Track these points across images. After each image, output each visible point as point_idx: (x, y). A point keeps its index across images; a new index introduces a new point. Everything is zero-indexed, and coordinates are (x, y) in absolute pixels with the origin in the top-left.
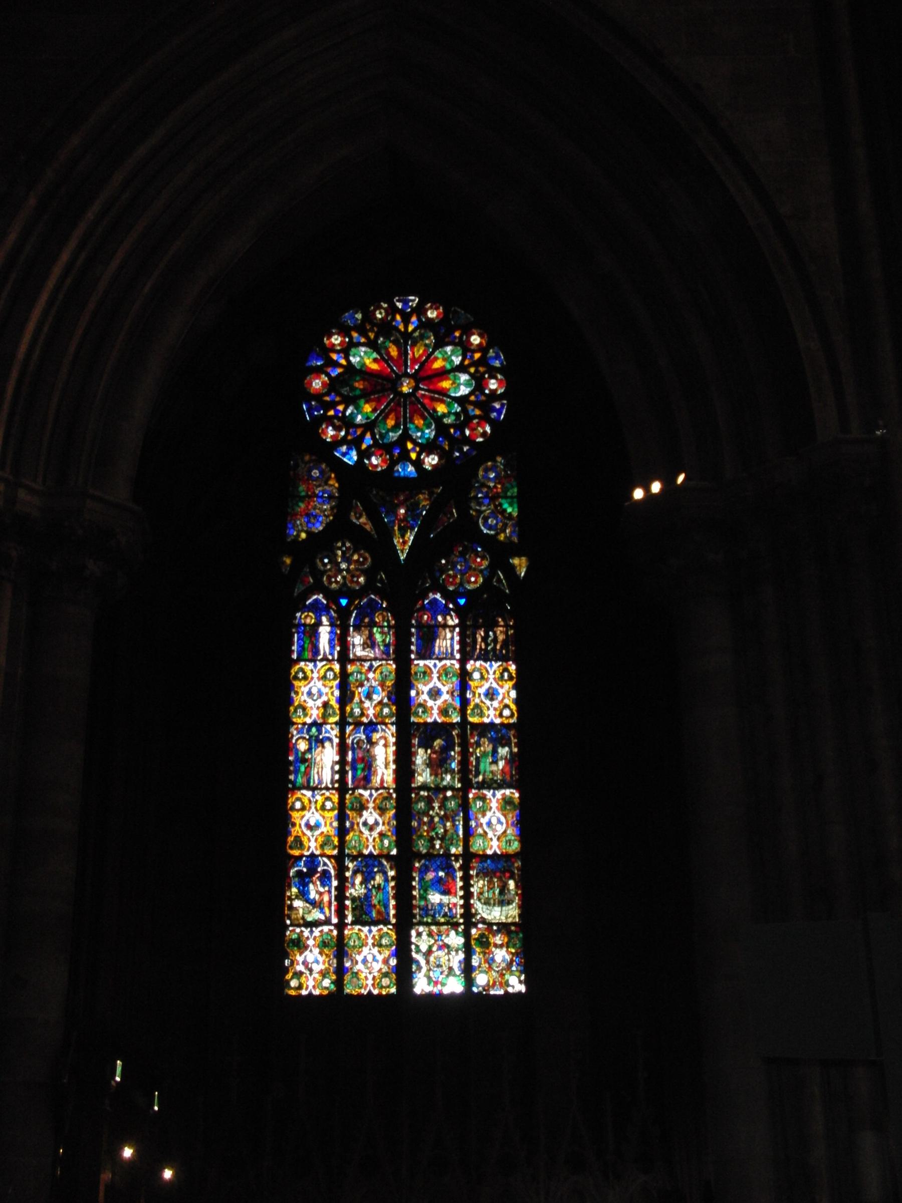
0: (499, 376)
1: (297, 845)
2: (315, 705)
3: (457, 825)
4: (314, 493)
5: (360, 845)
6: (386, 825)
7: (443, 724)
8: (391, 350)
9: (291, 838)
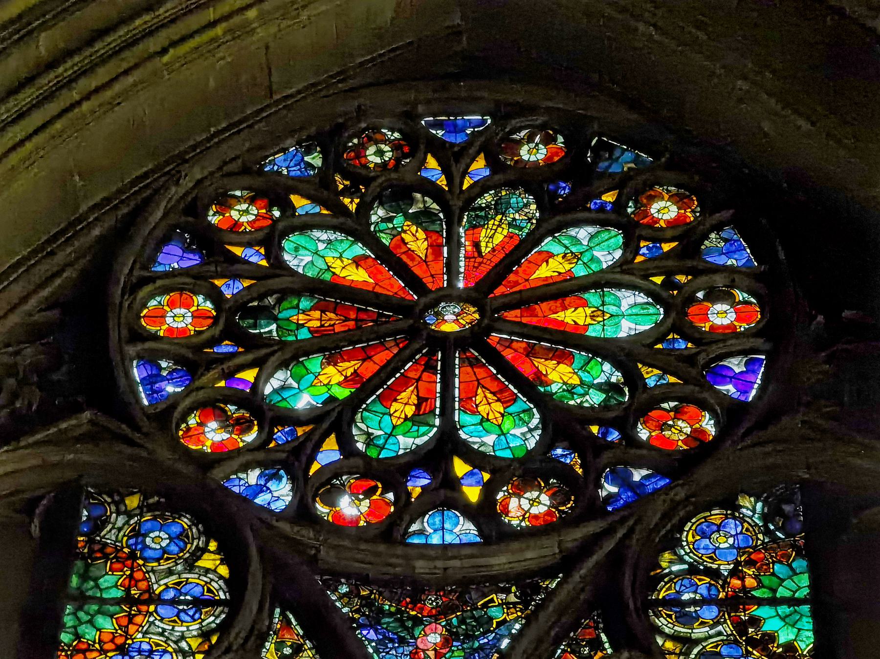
0: (740, 296)
4: (149, 590)
8: (407, 237)
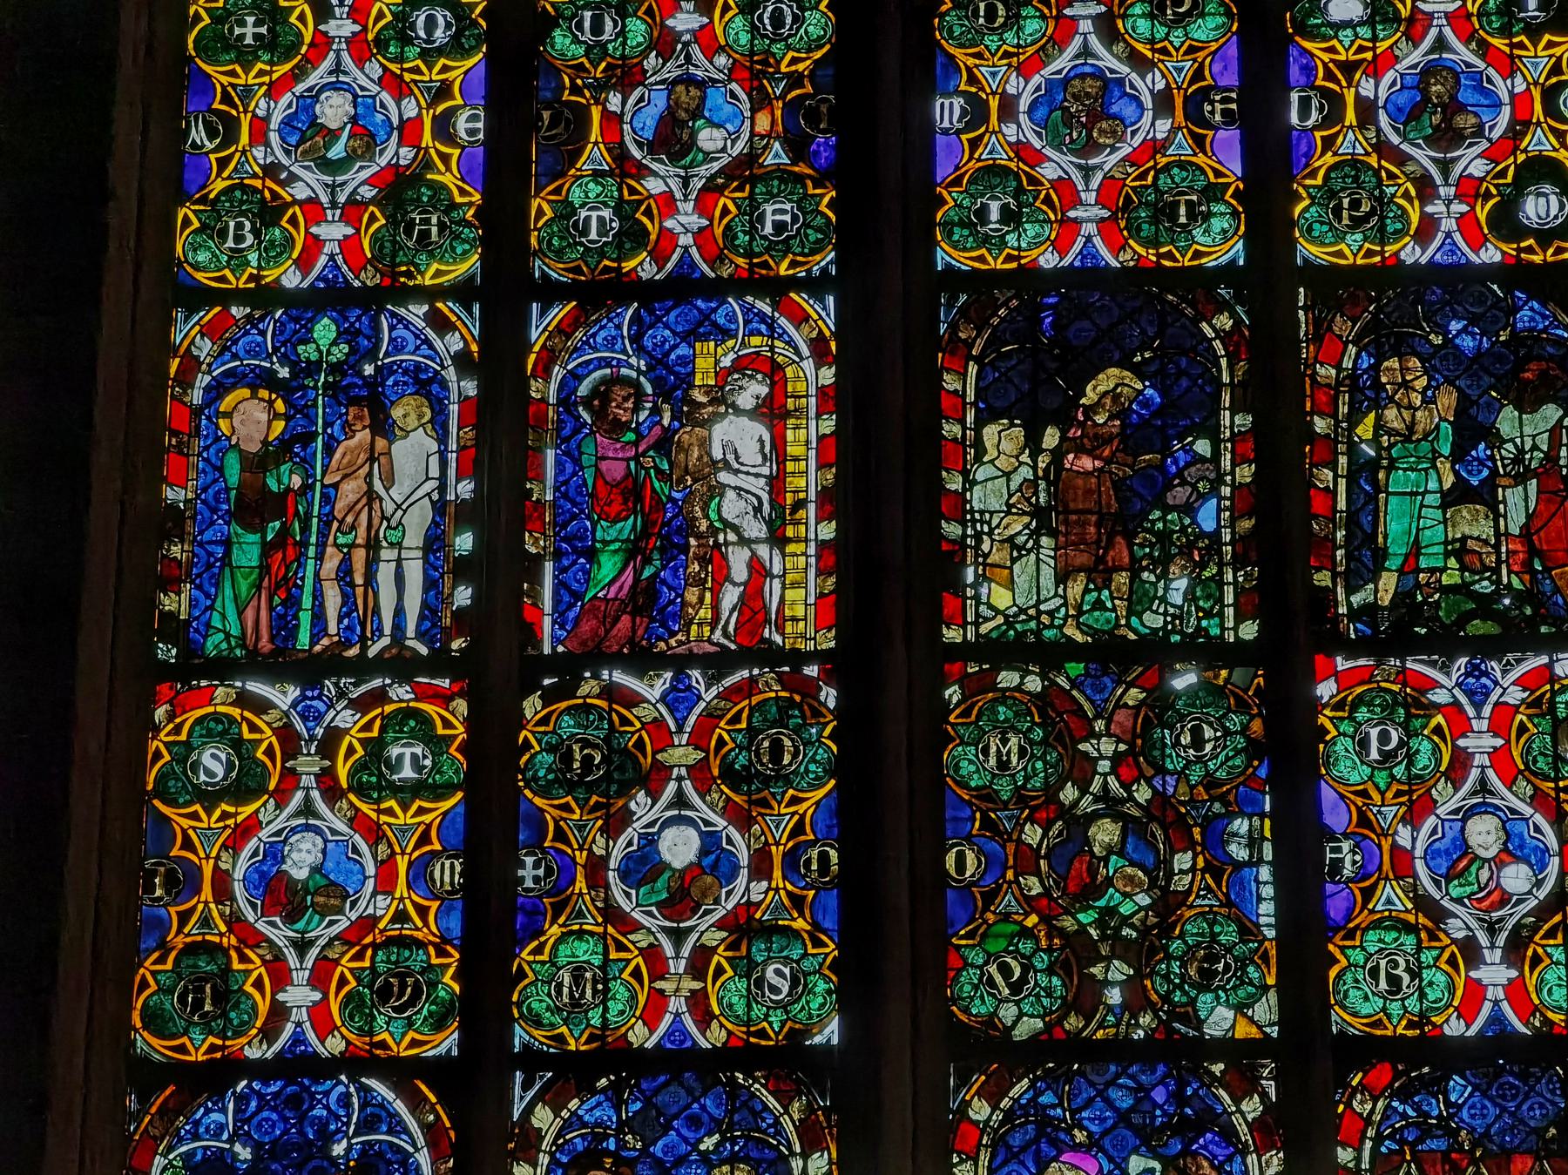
1: (198, 1004)
2: (333, 189)
3: (1238, 866)
5: (604, 996)
6: (777, 873)
7: (1138, 274)
9: (161, 960)
